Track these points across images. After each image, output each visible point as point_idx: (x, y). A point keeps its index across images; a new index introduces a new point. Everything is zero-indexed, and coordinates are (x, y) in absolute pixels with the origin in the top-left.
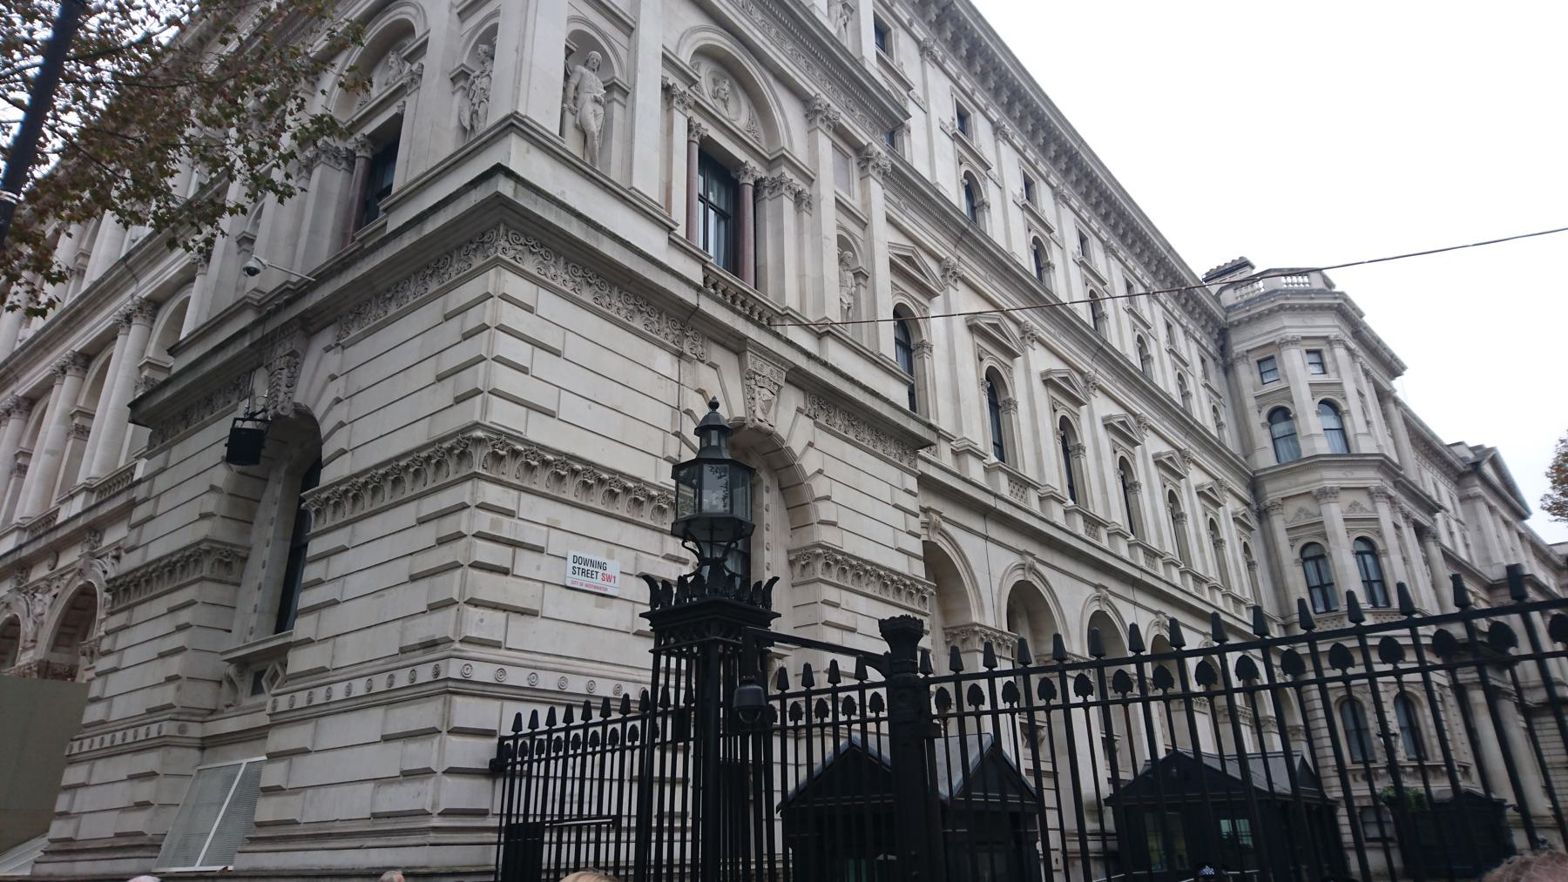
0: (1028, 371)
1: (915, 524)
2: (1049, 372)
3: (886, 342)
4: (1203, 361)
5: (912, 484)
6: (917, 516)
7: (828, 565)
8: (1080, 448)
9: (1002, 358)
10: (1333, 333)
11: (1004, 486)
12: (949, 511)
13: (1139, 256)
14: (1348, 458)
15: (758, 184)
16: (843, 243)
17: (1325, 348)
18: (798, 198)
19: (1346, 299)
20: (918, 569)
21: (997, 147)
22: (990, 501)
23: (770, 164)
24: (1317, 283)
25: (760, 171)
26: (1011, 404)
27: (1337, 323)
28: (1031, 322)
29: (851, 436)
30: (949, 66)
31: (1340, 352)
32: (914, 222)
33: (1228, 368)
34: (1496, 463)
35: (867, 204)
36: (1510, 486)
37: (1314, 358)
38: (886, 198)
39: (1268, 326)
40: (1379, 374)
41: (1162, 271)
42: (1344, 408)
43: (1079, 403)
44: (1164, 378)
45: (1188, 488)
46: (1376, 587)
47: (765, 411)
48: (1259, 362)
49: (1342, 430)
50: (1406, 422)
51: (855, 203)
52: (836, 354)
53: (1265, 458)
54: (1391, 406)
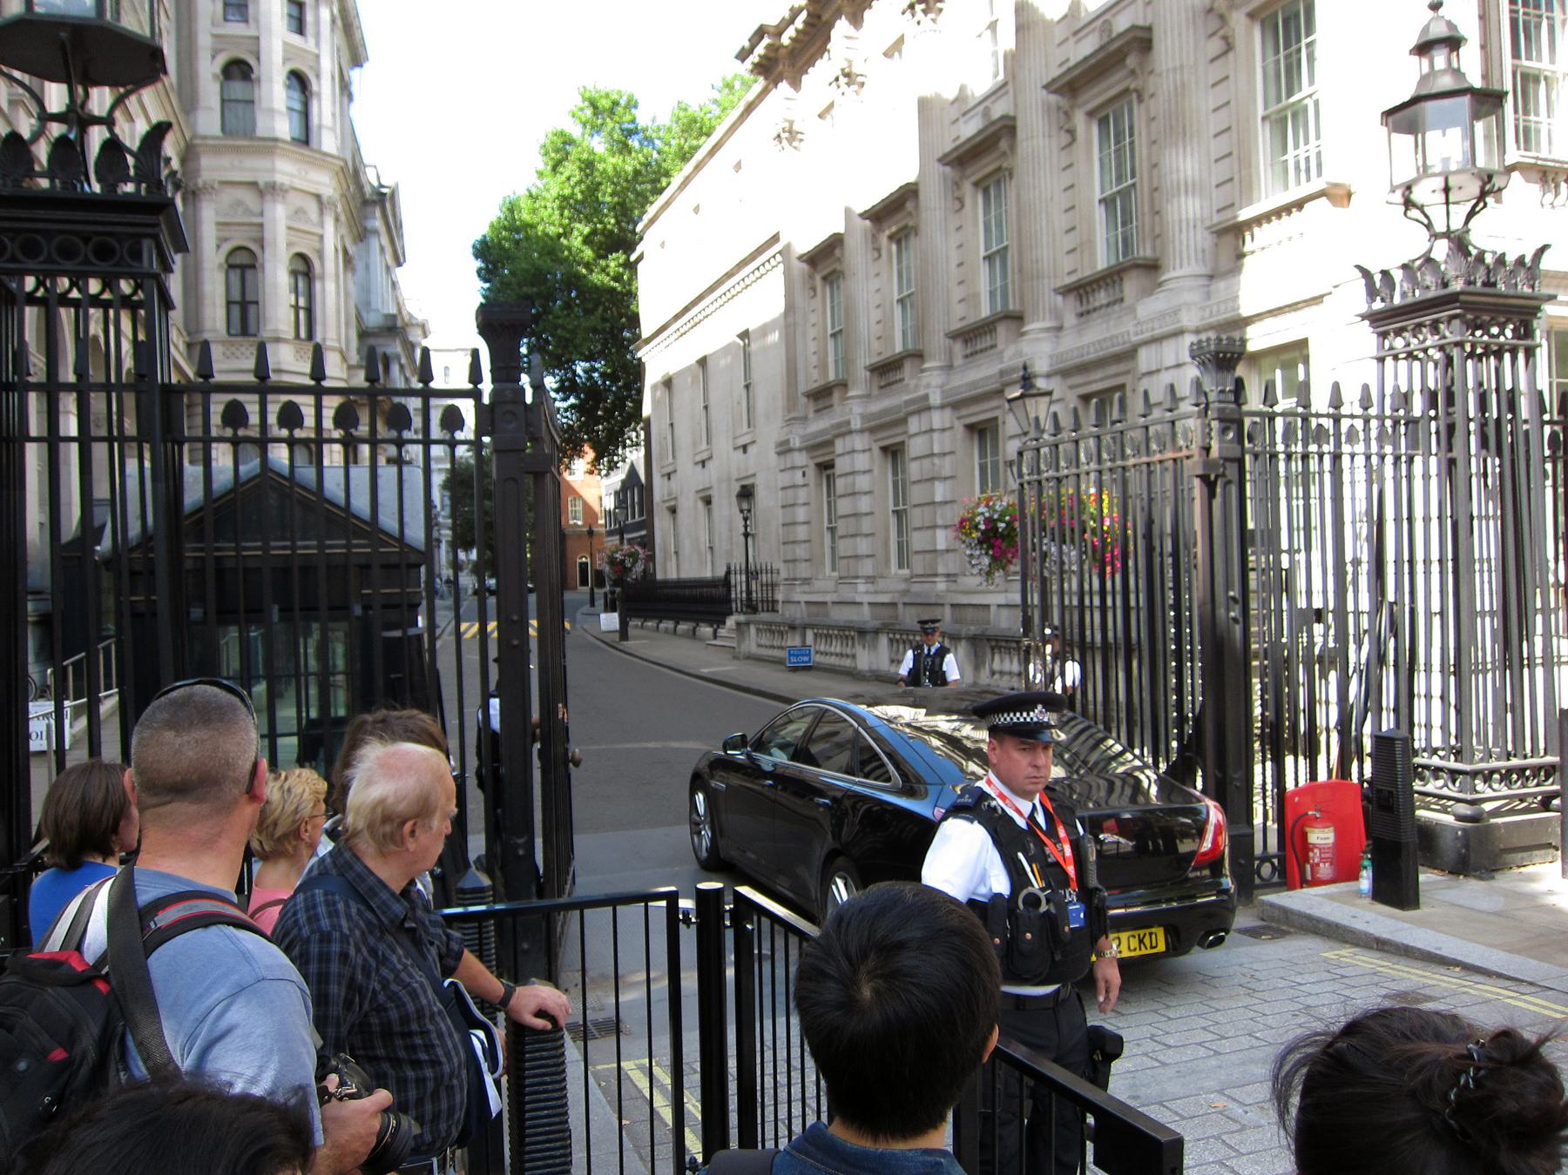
34: (393, 195)
36: (399, 227)
42: (315, 88)
46: (302, 314)
49: (306, 114)
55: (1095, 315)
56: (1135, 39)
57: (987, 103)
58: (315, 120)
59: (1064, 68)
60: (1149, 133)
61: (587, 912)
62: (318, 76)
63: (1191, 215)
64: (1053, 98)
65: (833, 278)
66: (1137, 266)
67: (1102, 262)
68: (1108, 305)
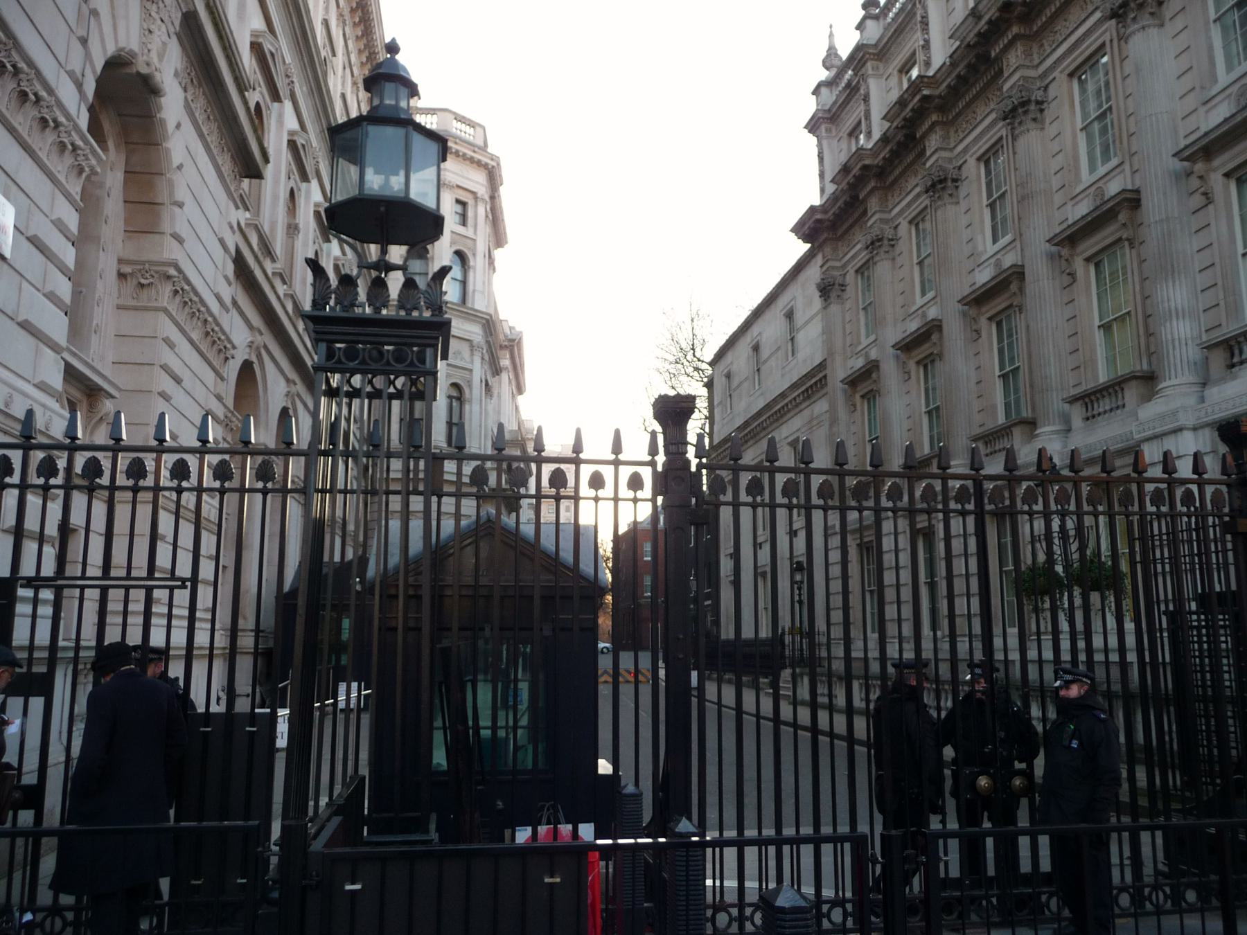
17: (471, 202)
19: (498, 164)
31: (481, 210)
34: (519, 343)
36: (522, 365)
37: (459, 208)
42: (472, 263)
55: (1100, 418)
56: (1126, 199)
57: (998, 256)
58: (470, 287)
59: (1065, 225)
60: (1141, 272)
61: (802, 846)
62: (474, 255)
63: (1183, 336)
64: (1054, 249)
65: (871, 397)
66: (1136, 378)
67: (1103, 377)
68: (1111, 410)
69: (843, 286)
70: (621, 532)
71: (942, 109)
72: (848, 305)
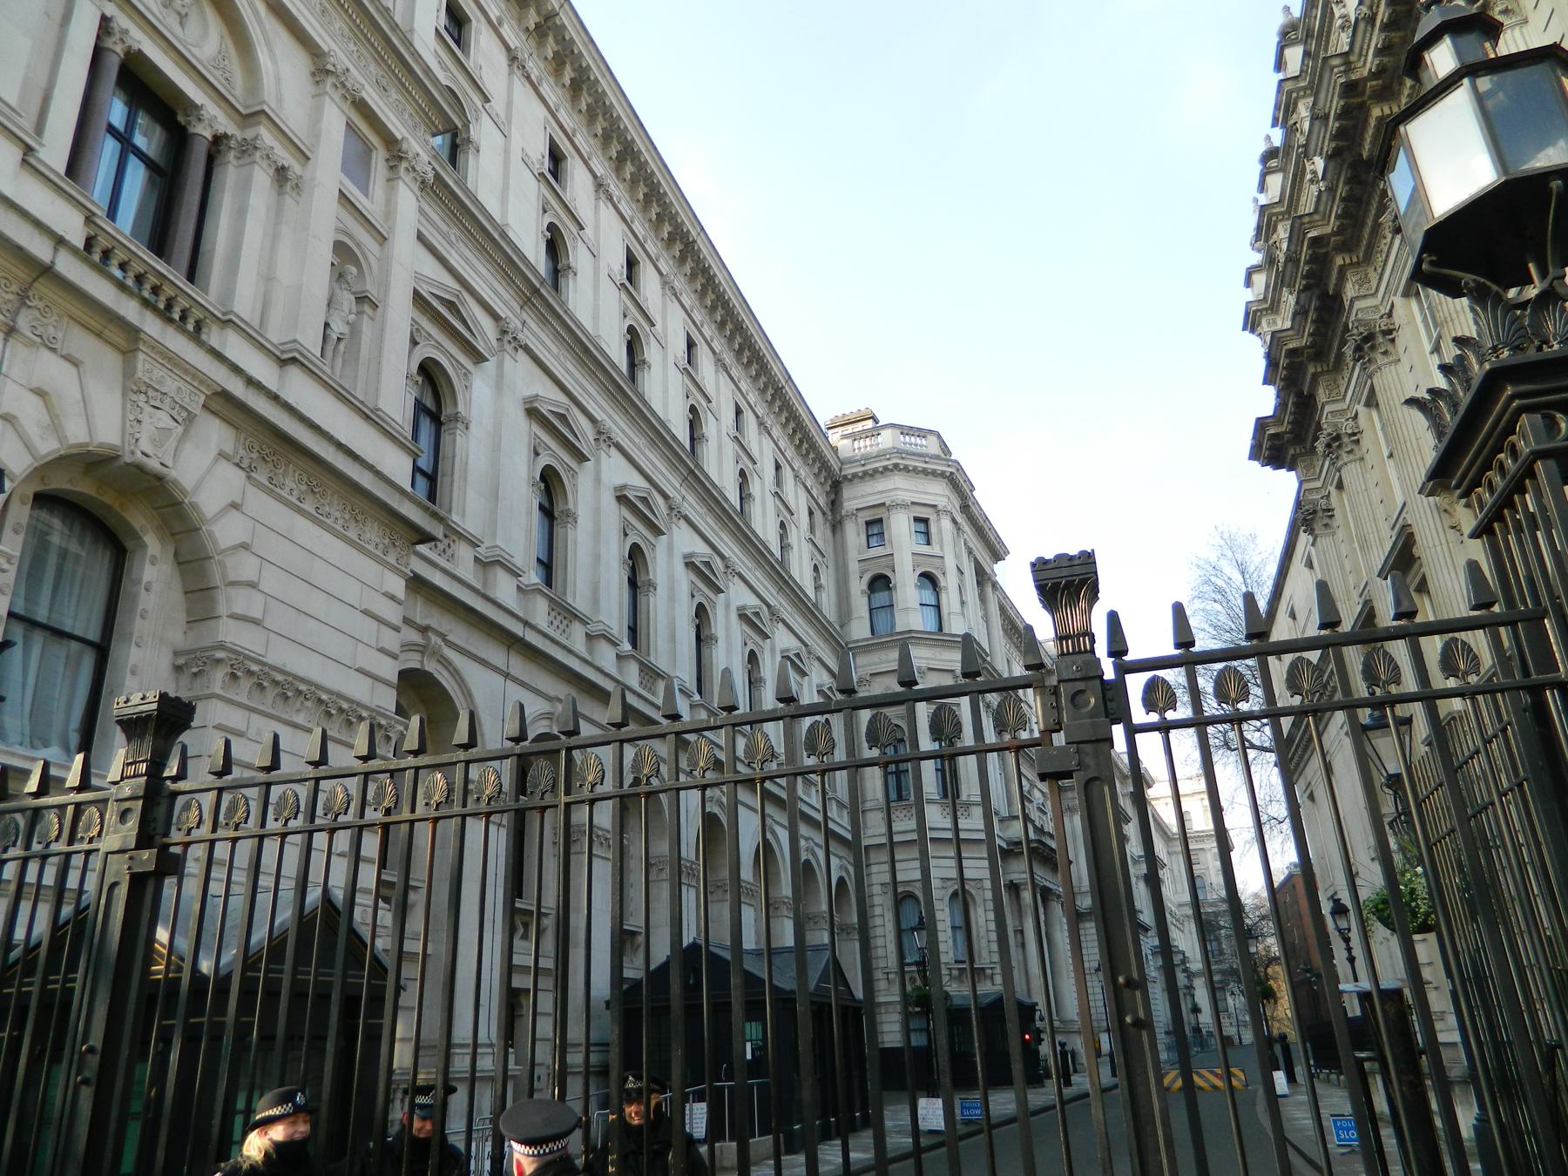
0: (598, 479)
1: (391, 640)
2: (624, 487)
3: (397, 398)
4: (811, 513)
5: (398, 586)
6: (397, 629)
7: (234, 676)
8: (651, 585)
9: (567, 458)
10: (942, 502)
11: (540, 612)
12: (459, 633)
13: (755, 378)
14: (938, 636)
15: (219, 140)
16: (343, 251)
17: (933, 518)
18: (281, 173)
19: (960, 469)
20: (387, 700)
21: (596, 207)
22: (516, 628)
23: (249, 118)
24: (931, 446)
25: (224, 123)
26: (570, 516)
27: (947, 492)
28: (609, 423)
29: (308, 506)
30: (545, 89)
31: (946, 523)
32: (467, 261)
33: (836, 526)
35: (390, 212)
37: (922, 527)
38: (421, 211)
39: (882, 484)
40: (983, 556)
41: (778, 403)
43: (657, 531)
44: (764, 523)
45: (773, 650)
47: (158, 443)
48: (868, 523)
49: (938, 607)
50: (1002, 609)
51: (372, 206)
52: (300, 391)
53: (859, 629)
54: (989, 589)
58: (945, 611)
69: (1329, 510)
70: (1278, 879)
71: (1347, 247)
72: (1340, 534)
